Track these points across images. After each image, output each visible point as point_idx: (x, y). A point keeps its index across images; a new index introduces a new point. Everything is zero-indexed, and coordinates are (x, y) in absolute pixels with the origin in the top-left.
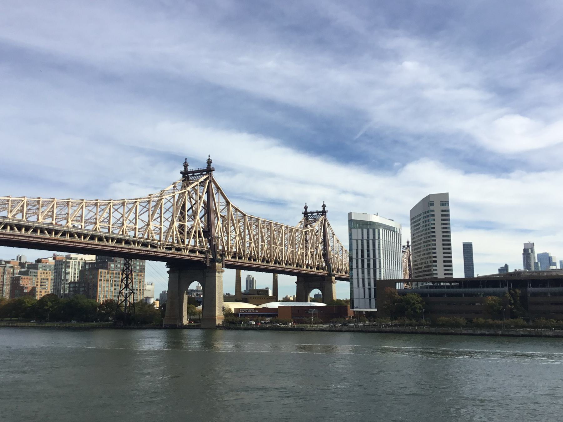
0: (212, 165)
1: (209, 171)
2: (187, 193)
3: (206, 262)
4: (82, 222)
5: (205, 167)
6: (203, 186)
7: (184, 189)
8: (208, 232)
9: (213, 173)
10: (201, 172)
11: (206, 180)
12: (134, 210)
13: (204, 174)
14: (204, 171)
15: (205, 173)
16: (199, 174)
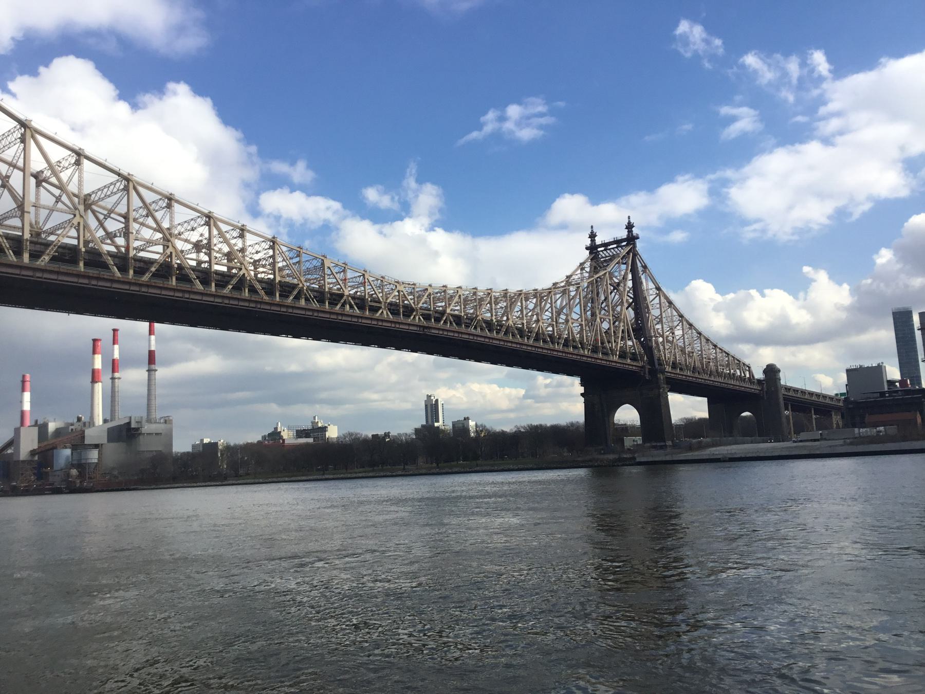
0: (635, 231)
1: (631, 239)
2: (607, 274)
3: (645, 373)
4: (523, 320)
5: (624, 234)
6: (625, 264)
7: (604, 270)
8: (640, 329)
9: (637, 241)
10: (618, 242)
11: (628, 253)
12: (549, 301)
13: (624, 246)
14: (622, 240)
15: (624, 243)
16: (615, 246)
